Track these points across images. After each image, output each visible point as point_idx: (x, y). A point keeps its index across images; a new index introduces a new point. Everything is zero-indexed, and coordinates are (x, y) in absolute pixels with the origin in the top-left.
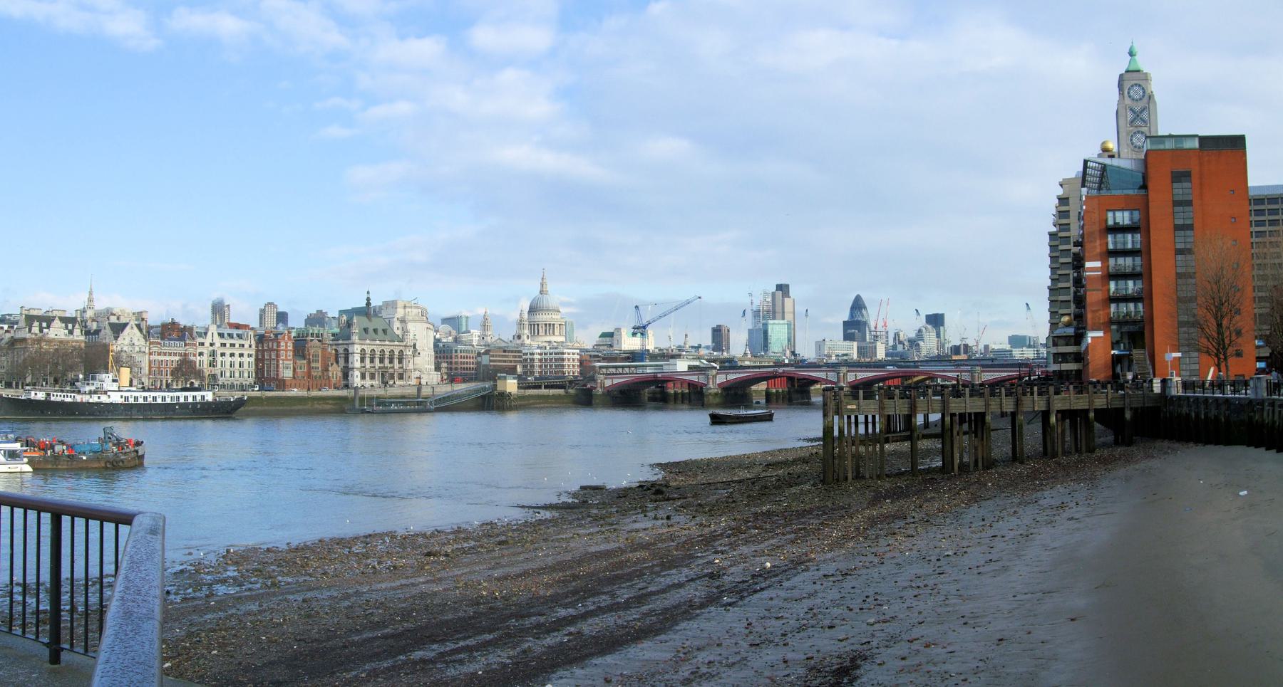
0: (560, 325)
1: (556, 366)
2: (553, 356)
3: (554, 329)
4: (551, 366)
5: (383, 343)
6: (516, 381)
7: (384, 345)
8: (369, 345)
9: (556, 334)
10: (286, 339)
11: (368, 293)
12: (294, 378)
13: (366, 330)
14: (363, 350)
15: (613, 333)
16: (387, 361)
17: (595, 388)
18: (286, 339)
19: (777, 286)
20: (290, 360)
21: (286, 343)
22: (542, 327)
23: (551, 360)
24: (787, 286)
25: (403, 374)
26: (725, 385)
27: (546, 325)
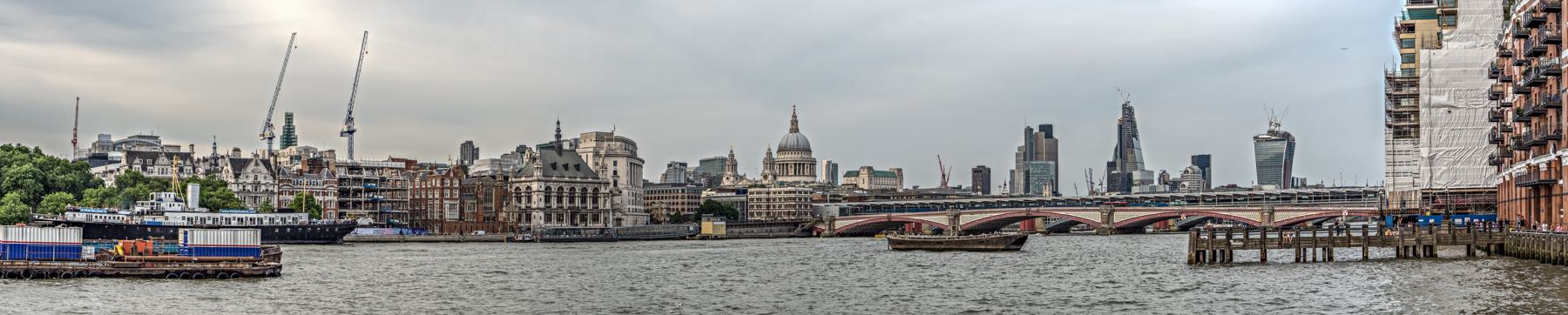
1: (786, 206)
2: (783, 195)
3: (804, 168)
5: (573, 180)
6: (724, 223)
7: (575, 182)
8: (556, 181)
10: (452, 175)
11: (558, 123)
12: (460, 219)
13: (554, 166)
14: (561, 189)
15: (859, 172)
16: (578, 202)
18: (452, 175)
19: (1040, 126)
20: (456, 199)
21: (451, 180)
23: (780, 199)
24: (1050, 127)
25: (598, 215)
26: (966, 227)
27: (795, 164)
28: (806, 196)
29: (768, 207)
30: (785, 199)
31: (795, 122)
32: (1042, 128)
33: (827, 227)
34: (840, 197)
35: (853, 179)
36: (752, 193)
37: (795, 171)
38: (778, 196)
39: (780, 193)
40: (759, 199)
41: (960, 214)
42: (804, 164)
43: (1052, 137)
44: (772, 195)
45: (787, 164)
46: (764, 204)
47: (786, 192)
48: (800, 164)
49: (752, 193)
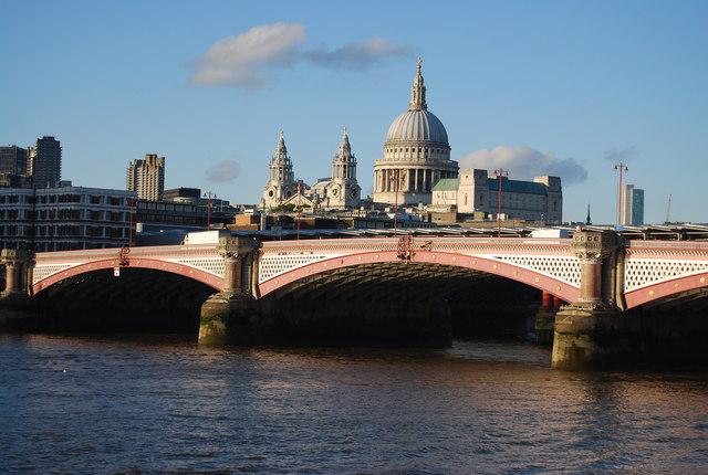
23: (52, 214)
27: (412, 171)
30: (63, 214)
37: (412, 182)
38: (50, 207)
39: (53, 199)
40: (13, 214)
42: (429, 172)
44: (40, 207)
48: (421, 171)
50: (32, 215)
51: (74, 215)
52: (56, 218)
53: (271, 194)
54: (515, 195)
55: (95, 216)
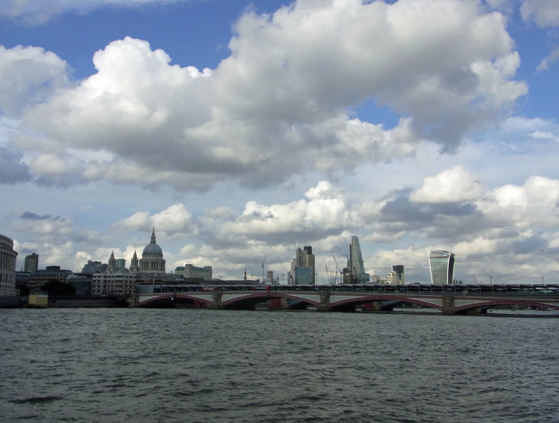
0: (161, 263)
1: (116, 286)
3: (157, 266)
4: (112, 286)
6: (46, 296)
9: (158, 268)
17: (131, 303)
22: (150, 264)
23: (113, 281)
27: (152, 263)
28: (131, 279)
29: (105, 286)
30: (117, 281)
31: (153, 237)
32: (306, 248)
33: (134, 301)
34: (162, 281)
35: (181, 271)
36: (95, 277)
37: (152, 266)
38: (111, 279)
39: (113, 277)
40: (99, 281)
41: (222, 294)
42: (157, 263)
43: (312, 254)
44: (108, 279)
45: (147, 263)
46: (102, 285)
47: (116, 277)
48: (155, 263)
49: (95, 277)
50: (105, 281)
51: (121, 281)
52: (114, 282)
53: (109, 270)
54: (200, 272)
55: (126, 281)
